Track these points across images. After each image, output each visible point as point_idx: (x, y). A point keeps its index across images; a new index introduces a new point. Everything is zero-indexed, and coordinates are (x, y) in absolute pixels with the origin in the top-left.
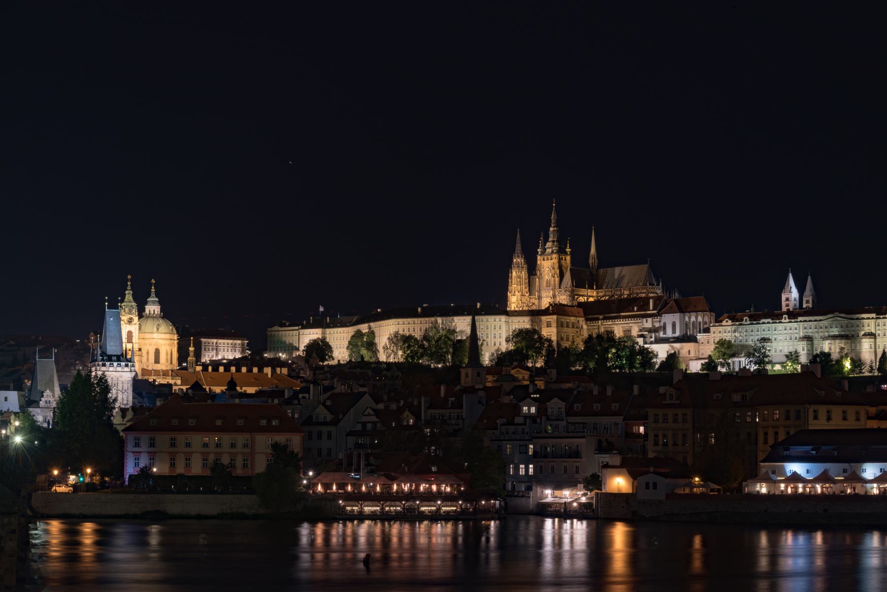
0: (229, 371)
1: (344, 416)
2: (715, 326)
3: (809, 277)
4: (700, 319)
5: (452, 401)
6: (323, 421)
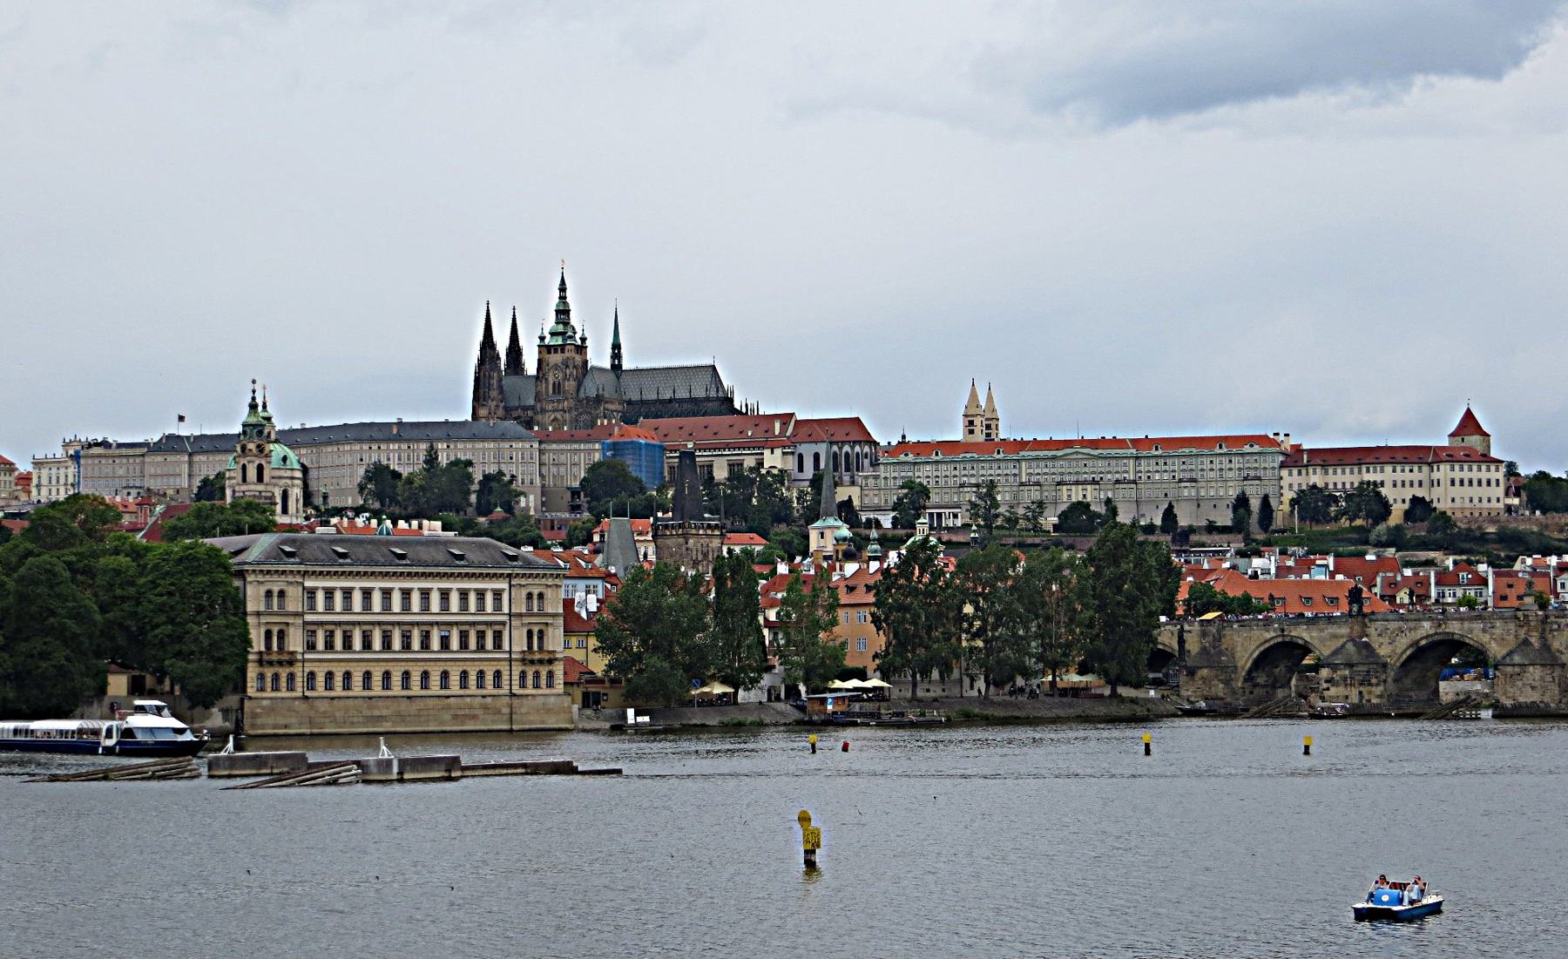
4: (857, 449)
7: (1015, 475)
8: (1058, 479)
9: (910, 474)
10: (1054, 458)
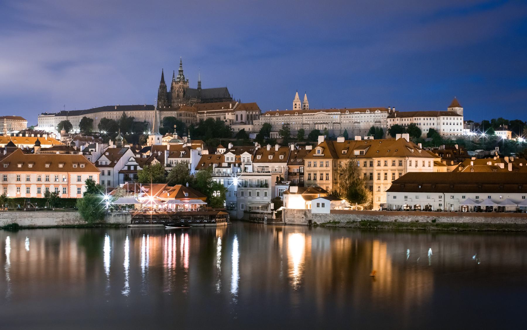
0: (25, 136)
1: (117, 162)
2: (262, 117)
3: (306, 94)
4: (254, 113)
5: (183, 153)
6: (105, 164)
7: (302, 121)
8: (316, 122)
9: (269, 121)
10: (314, 115)
